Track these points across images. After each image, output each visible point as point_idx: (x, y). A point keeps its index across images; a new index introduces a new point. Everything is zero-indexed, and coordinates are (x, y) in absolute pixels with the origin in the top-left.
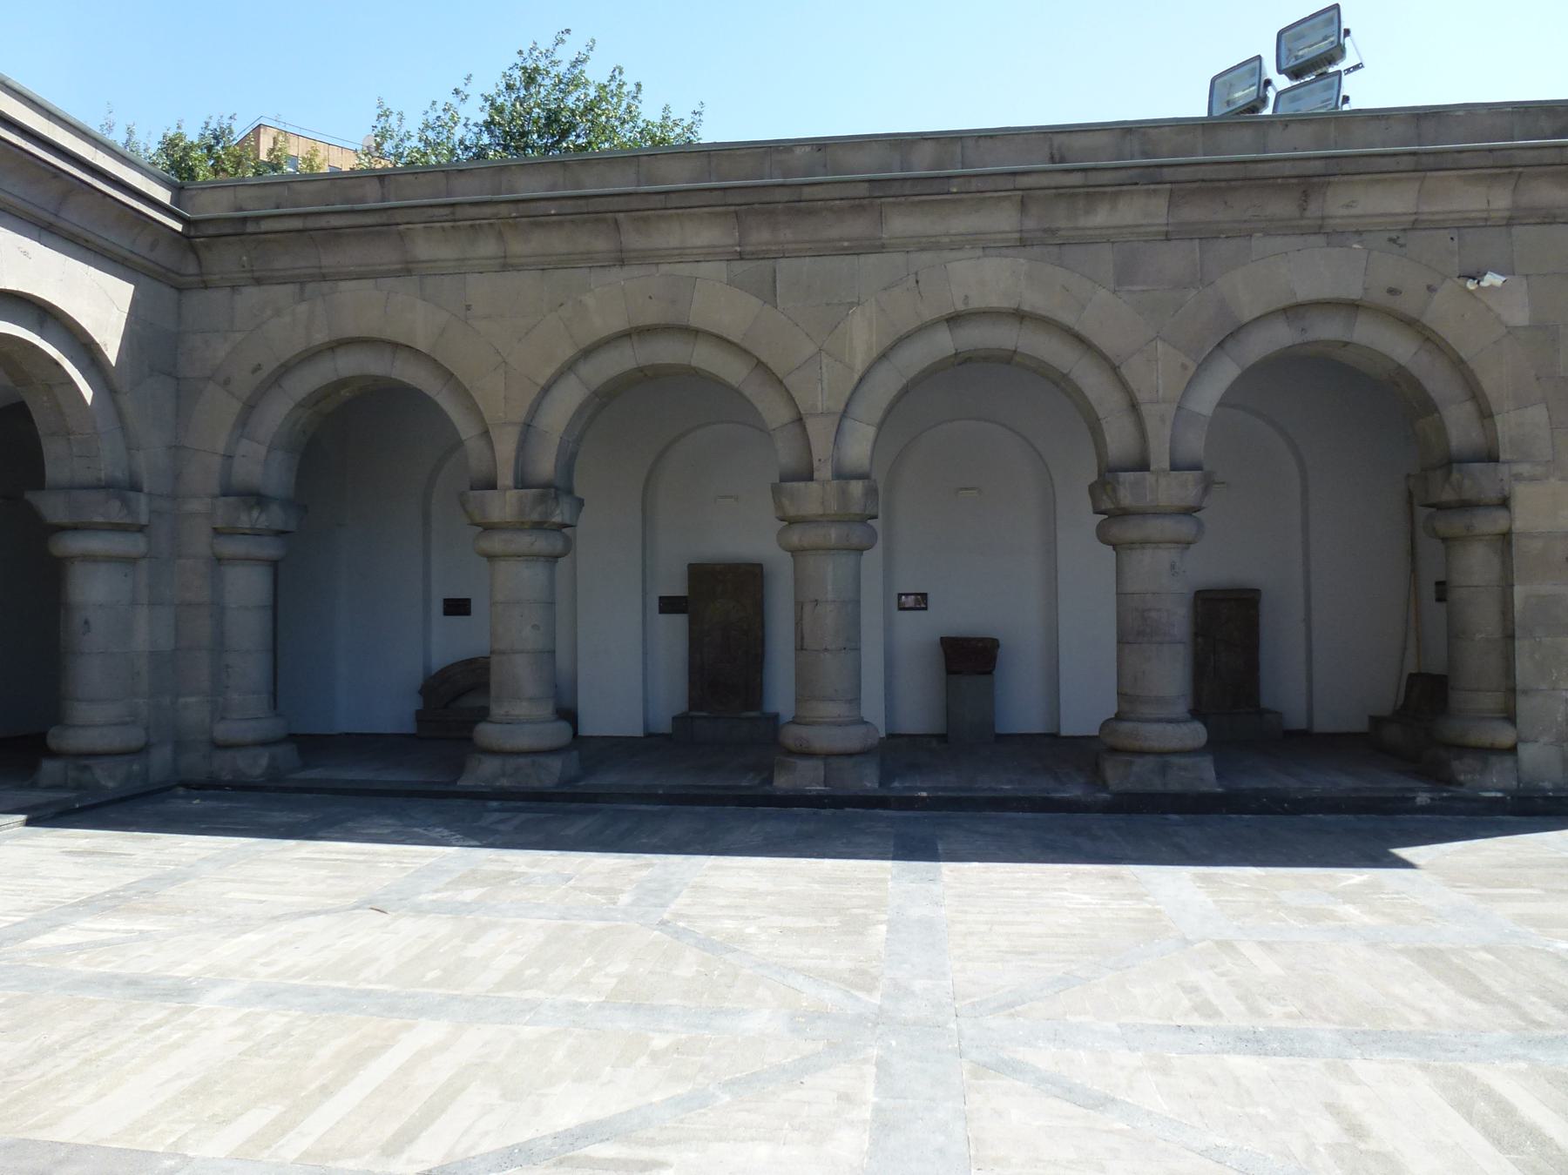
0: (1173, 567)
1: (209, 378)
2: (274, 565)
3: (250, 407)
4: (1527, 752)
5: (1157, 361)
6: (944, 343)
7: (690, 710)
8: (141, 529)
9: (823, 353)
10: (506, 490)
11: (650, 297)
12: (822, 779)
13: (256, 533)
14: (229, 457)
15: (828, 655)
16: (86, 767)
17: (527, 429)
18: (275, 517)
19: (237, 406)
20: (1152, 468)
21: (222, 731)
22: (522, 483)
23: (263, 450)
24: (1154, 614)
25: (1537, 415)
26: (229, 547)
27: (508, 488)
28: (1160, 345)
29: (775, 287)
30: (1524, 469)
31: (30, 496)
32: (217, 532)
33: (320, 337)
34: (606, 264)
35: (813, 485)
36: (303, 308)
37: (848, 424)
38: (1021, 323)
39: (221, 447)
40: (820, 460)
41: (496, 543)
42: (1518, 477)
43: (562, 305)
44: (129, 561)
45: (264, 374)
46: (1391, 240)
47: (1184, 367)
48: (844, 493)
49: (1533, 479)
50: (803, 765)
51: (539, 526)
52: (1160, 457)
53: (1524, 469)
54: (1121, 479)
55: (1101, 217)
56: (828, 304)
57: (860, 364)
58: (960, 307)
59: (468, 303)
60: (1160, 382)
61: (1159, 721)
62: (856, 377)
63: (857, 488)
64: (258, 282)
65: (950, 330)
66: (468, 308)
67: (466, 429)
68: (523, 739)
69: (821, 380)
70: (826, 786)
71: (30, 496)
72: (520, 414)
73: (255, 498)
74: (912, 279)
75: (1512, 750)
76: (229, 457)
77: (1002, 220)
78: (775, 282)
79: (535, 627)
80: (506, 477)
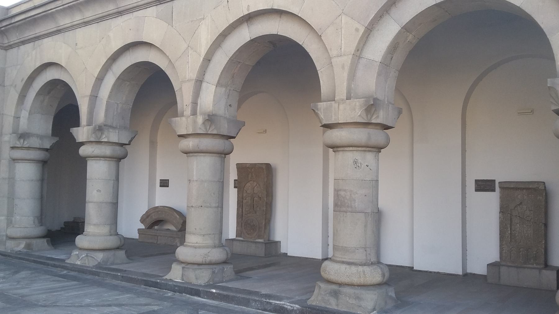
0: (355, 162)
1: (12, 85)
3: (22, 96)
5: (341, 29)
7: (236, 236)
9: (189, 48)
10: (84, 127)
11: (130, 29)
12: (181, 276)
13: (29, 148)
15: (193, 209)
17: (94, 98)
18: (35, 142)
20: (336, 99)
22: (89, 124)
24: (342, 193)
26: (18, 154)
27: (84, 126)
28: (344, 17)
29: (173, 16)
33: (38, 64)
34: (116, 16)
36: (34, 52)
37: (204, 85)
38: (280, 17)
39: (13, 114)
40: (186, 105)
43: (103, 38)
45: (24, 81)
47: (357, 30)
48: (195, 122)
51: (99, 142)
54: (319, 107)
56: (192, 21)
58: (246, 13)
59: (76, 43)
60: (343, 42)
61: (343, 262)
63: (200, 120)
65: (248, 26)
66: (76, 44)
69: (188, 62)
70: (182, 281)
72: (88, 91)
78: (172, 13)
79: (99, 191)
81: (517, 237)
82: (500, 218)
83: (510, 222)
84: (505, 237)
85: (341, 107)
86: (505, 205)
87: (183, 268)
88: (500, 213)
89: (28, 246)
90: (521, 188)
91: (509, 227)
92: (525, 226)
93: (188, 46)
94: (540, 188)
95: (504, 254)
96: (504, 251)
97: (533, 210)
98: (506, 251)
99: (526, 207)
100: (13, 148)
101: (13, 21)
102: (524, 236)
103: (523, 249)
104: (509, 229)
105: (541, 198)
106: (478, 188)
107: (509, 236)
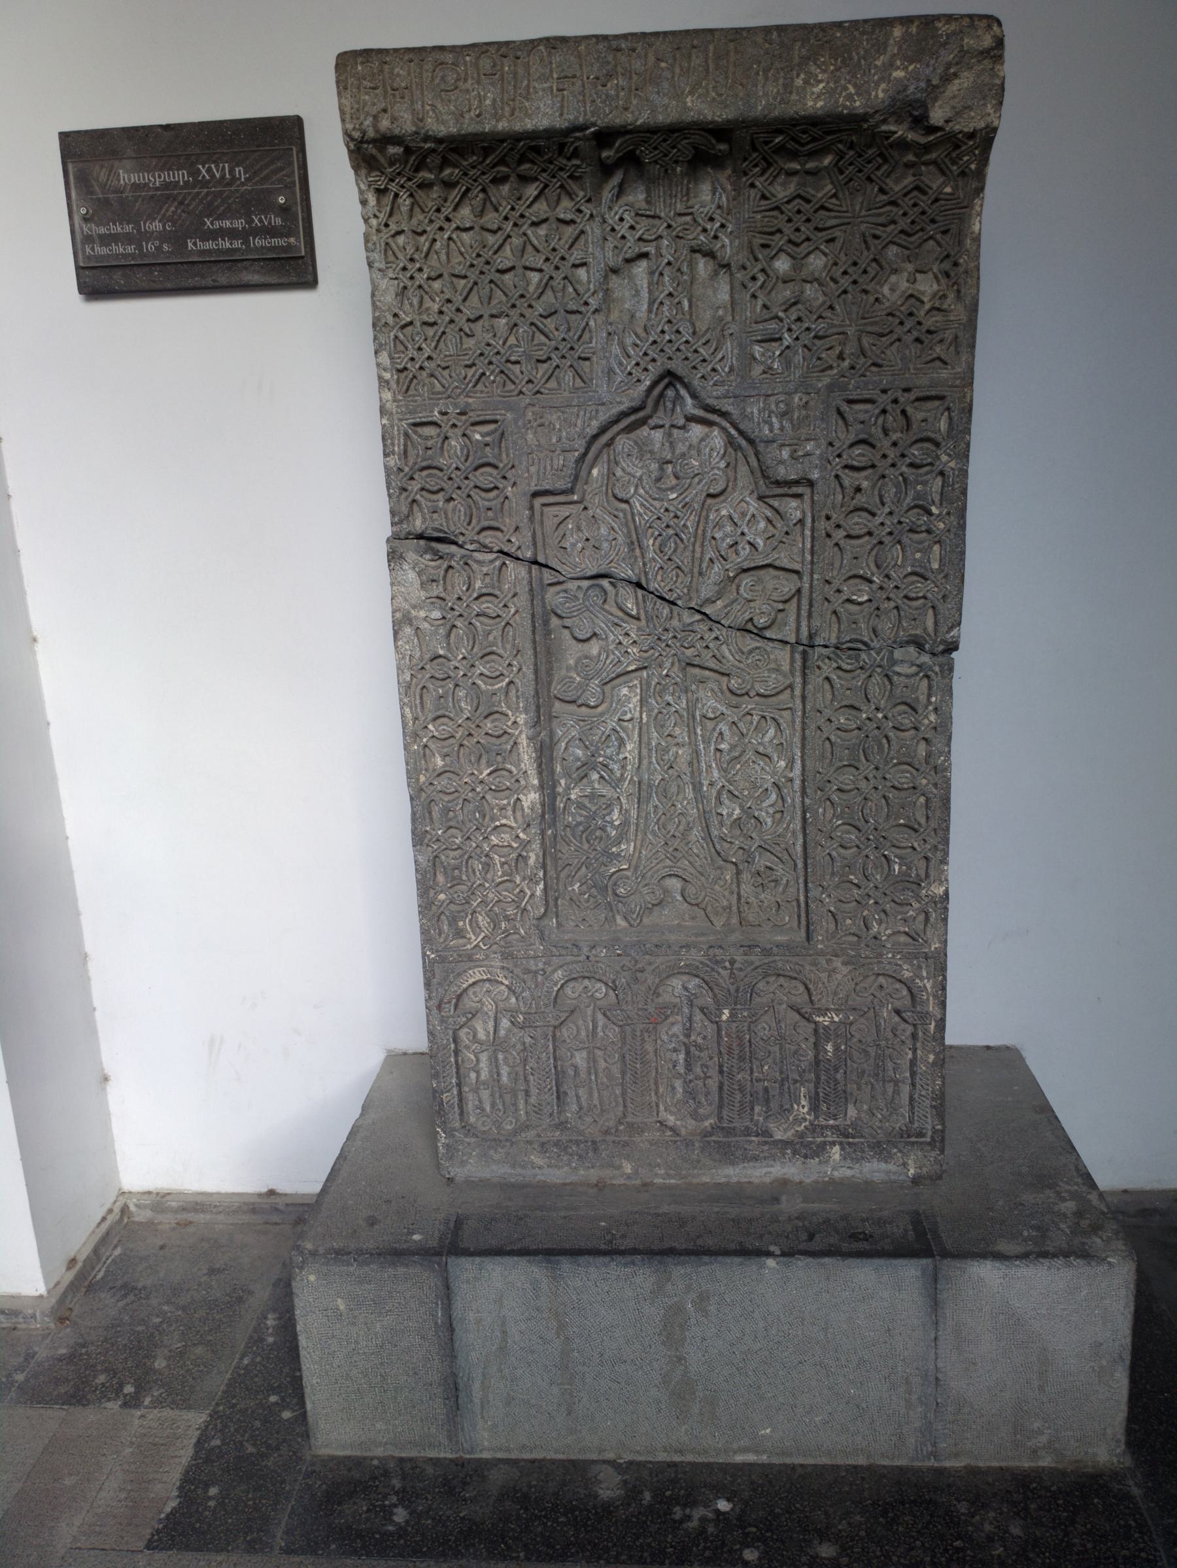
81: (628, 848)
82: (401, 622)
83: (528, 672)
84: (487, 867)
86: (455, 443)
88: (394, 557)
90: (674, 131)
91: (523, 740)
92: (710, 703)
94: (937, 115)
95: (484, 1064)
96: (483, 1029)
97: (815, 475)
98: (505, 1023)
99: (717, 439)
102: (696, 833)
103: (693, 983)
104: (527, 757)
105: (927, 286)
106: (106, 240)
107: (525, 845)
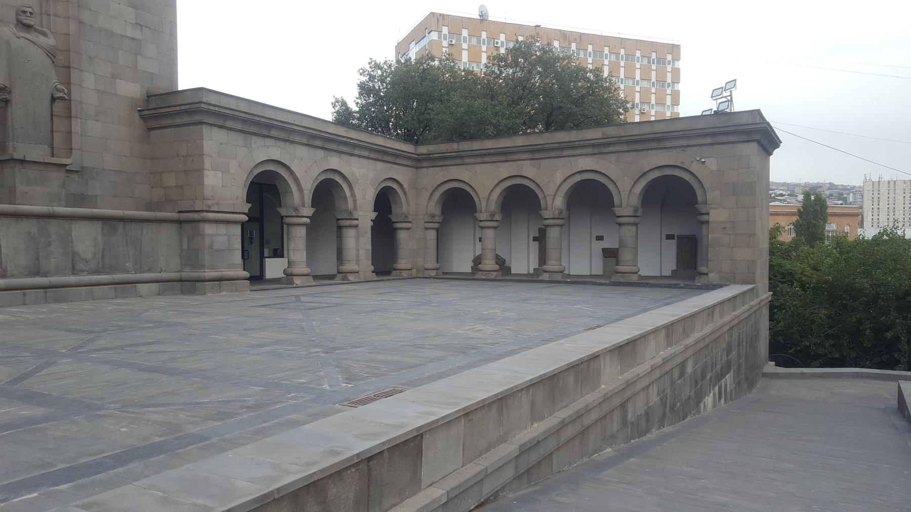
0: (629, 230)
2: (437, 230)
3: (432, 195)
4: (711, 275)
6: (578, 178)
8: (410, 222)
14: (427, 206)
16: (401, 272)
17: (488, 199)
18: (437, 219)
19: (429, 195)
21: (427, 266)
23: (434, 204)
24: (624, 241)
25: (717, 193)
28: (626, 178)
30: (713, 206)
31: (389, 216)
32: (425, 222)
35: (548, 211)
36: (442, 172)
37: (556, 197)
39: (426, 205)
41: (482, 224)
42: (711, 208)
44: (409, 229)
46: (683, 150)
49: (715, 208)
50: (544, 274)
52: (624, 205)
53: (713, 206)
55: (611, 149)
57: (558, 185)
58: (581, 170)
62: (557, 186)
63: (557, 212)
64: (433, 167)
66: (476, 172)
67: (476, 199)
68: (487, 269)
71: (389, 216)
72: (486, 196)
73: (433, 216)
74: (570, 164)
75: (708, 274)
76: (427, 206)
77: (590, 151)
79: (490, 243)
80: (484, 210)
85: (625, 210)
87: (549, 274)
89: (437, 273)
93: (550, 181)
100: (425, 222)
101: (431, 156)
